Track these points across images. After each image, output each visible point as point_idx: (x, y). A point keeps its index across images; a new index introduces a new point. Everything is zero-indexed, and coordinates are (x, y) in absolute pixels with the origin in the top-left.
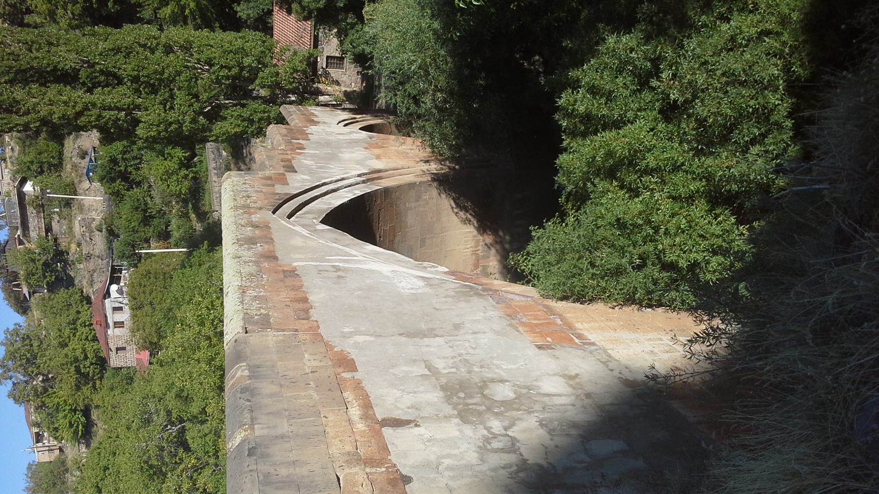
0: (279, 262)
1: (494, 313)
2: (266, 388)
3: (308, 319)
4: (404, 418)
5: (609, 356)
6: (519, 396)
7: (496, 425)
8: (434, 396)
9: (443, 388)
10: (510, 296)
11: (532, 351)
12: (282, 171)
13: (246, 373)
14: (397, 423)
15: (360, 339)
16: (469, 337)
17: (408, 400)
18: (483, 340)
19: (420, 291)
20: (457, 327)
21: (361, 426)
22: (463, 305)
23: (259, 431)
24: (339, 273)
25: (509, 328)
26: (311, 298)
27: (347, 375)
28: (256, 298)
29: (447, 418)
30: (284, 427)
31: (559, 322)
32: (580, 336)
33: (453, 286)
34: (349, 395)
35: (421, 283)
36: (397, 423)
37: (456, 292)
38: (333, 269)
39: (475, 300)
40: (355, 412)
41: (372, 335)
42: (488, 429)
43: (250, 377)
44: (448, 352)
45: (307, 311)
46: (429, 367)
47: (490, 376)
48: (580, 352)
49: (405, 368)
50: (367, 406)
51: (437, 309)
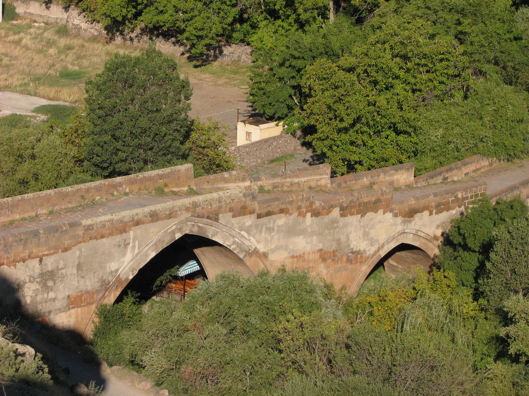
0: (133, 228)
1: (89, 288)
2: (57, 235)
3: (90, 239)
4: (42, 263)
5: (62, 312)
6: (48, 287)
7: (38, 280)
8: (50, 268)
9: (52, 271)
10: (101, 295)
11: (67, 293)
12: (258, 211)
13: (64, 229)
14: (41, 261)
15: (78, 253)
16: (76, 279)
17: (49, 263)
18: (75, 283)
19: (108, 269)
20: (83, 277)
21: (40, 254)
22: (96, 280)
23: (41, 236)
24: (123, 245)
25: (80, 290)
26: (104, 240)
27: (60, 250)
28: (104, 226)
29: (42, 271)
30: (42, 240)
31: (82, 304)
32: (73, 308)
33: (110, 279)
34: (52, 251)
35: (113, 269)
36: (41, 261)
37: (105, 280)
38: (126, 243)
39: (100, 284)
40: (46, 253)
41: (79, 255)
42: (37, 278)
43: (62, 231)
44: (68, 273)
45: (96, 238)
46: (62, 269)
47: (57, 282)
48: (65, 305)
49: (62, 263)
50: (47, 255)
51: (95, 273)
